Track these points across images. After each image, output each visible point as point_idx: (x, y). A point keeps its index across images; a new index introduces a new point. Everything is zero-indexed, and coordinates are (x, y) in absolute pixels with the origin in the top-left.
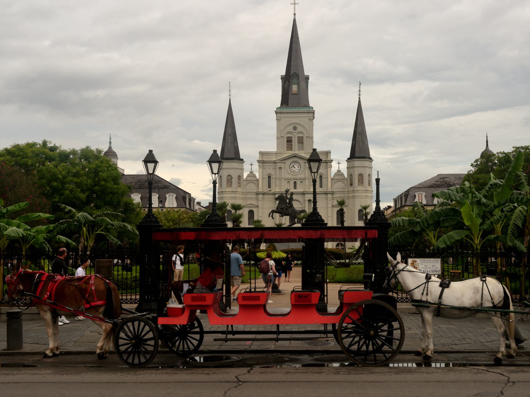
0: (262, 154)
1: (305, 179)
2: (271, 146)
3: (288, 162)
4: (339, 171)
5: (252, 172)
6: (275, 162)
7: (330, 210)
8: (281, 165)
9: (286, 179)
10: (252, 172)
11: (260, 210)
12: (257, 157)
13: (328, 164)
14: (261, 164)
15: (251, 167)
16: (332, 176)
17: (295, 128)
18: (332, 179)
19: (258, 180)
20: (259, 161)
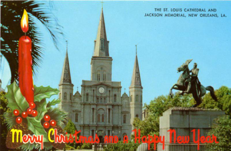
0: (84, 81)
1: (106, 97)
2: (88, 77)
3: (98, 87)
4: (125, 93)
5: (78, 92)
6: (91, 87)
7: (120, 114)
8: (95, 89)
9: (96, 97)
10: (78, 92)
11: (82, 114)
12: (81, 83)
13: (120, 89)
14: (83, 87)
15: (77, 88)
16: (121, 96)
17: (102, 68)
18: (121, 97)
19: (81, 96)
20: (82, 86)
